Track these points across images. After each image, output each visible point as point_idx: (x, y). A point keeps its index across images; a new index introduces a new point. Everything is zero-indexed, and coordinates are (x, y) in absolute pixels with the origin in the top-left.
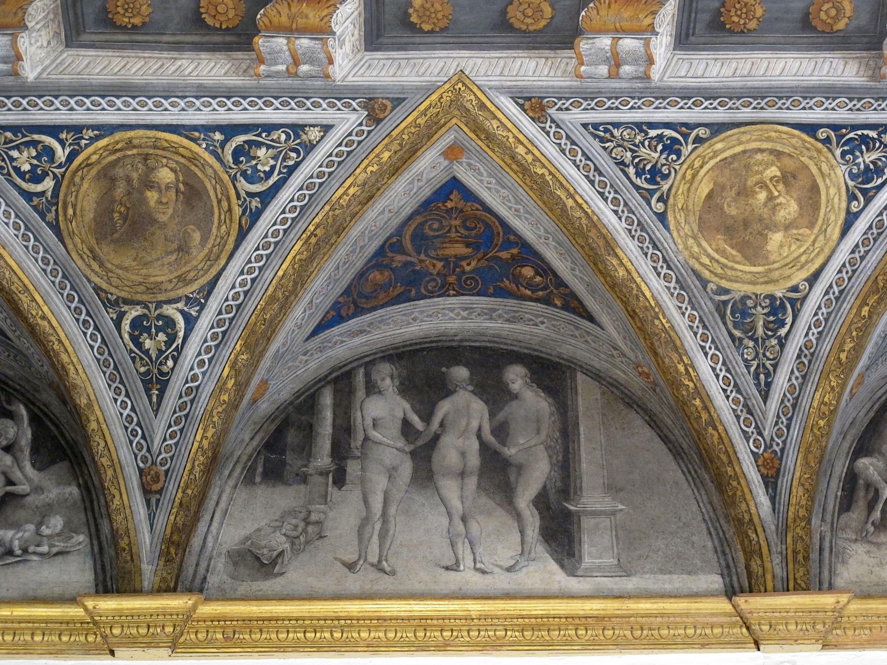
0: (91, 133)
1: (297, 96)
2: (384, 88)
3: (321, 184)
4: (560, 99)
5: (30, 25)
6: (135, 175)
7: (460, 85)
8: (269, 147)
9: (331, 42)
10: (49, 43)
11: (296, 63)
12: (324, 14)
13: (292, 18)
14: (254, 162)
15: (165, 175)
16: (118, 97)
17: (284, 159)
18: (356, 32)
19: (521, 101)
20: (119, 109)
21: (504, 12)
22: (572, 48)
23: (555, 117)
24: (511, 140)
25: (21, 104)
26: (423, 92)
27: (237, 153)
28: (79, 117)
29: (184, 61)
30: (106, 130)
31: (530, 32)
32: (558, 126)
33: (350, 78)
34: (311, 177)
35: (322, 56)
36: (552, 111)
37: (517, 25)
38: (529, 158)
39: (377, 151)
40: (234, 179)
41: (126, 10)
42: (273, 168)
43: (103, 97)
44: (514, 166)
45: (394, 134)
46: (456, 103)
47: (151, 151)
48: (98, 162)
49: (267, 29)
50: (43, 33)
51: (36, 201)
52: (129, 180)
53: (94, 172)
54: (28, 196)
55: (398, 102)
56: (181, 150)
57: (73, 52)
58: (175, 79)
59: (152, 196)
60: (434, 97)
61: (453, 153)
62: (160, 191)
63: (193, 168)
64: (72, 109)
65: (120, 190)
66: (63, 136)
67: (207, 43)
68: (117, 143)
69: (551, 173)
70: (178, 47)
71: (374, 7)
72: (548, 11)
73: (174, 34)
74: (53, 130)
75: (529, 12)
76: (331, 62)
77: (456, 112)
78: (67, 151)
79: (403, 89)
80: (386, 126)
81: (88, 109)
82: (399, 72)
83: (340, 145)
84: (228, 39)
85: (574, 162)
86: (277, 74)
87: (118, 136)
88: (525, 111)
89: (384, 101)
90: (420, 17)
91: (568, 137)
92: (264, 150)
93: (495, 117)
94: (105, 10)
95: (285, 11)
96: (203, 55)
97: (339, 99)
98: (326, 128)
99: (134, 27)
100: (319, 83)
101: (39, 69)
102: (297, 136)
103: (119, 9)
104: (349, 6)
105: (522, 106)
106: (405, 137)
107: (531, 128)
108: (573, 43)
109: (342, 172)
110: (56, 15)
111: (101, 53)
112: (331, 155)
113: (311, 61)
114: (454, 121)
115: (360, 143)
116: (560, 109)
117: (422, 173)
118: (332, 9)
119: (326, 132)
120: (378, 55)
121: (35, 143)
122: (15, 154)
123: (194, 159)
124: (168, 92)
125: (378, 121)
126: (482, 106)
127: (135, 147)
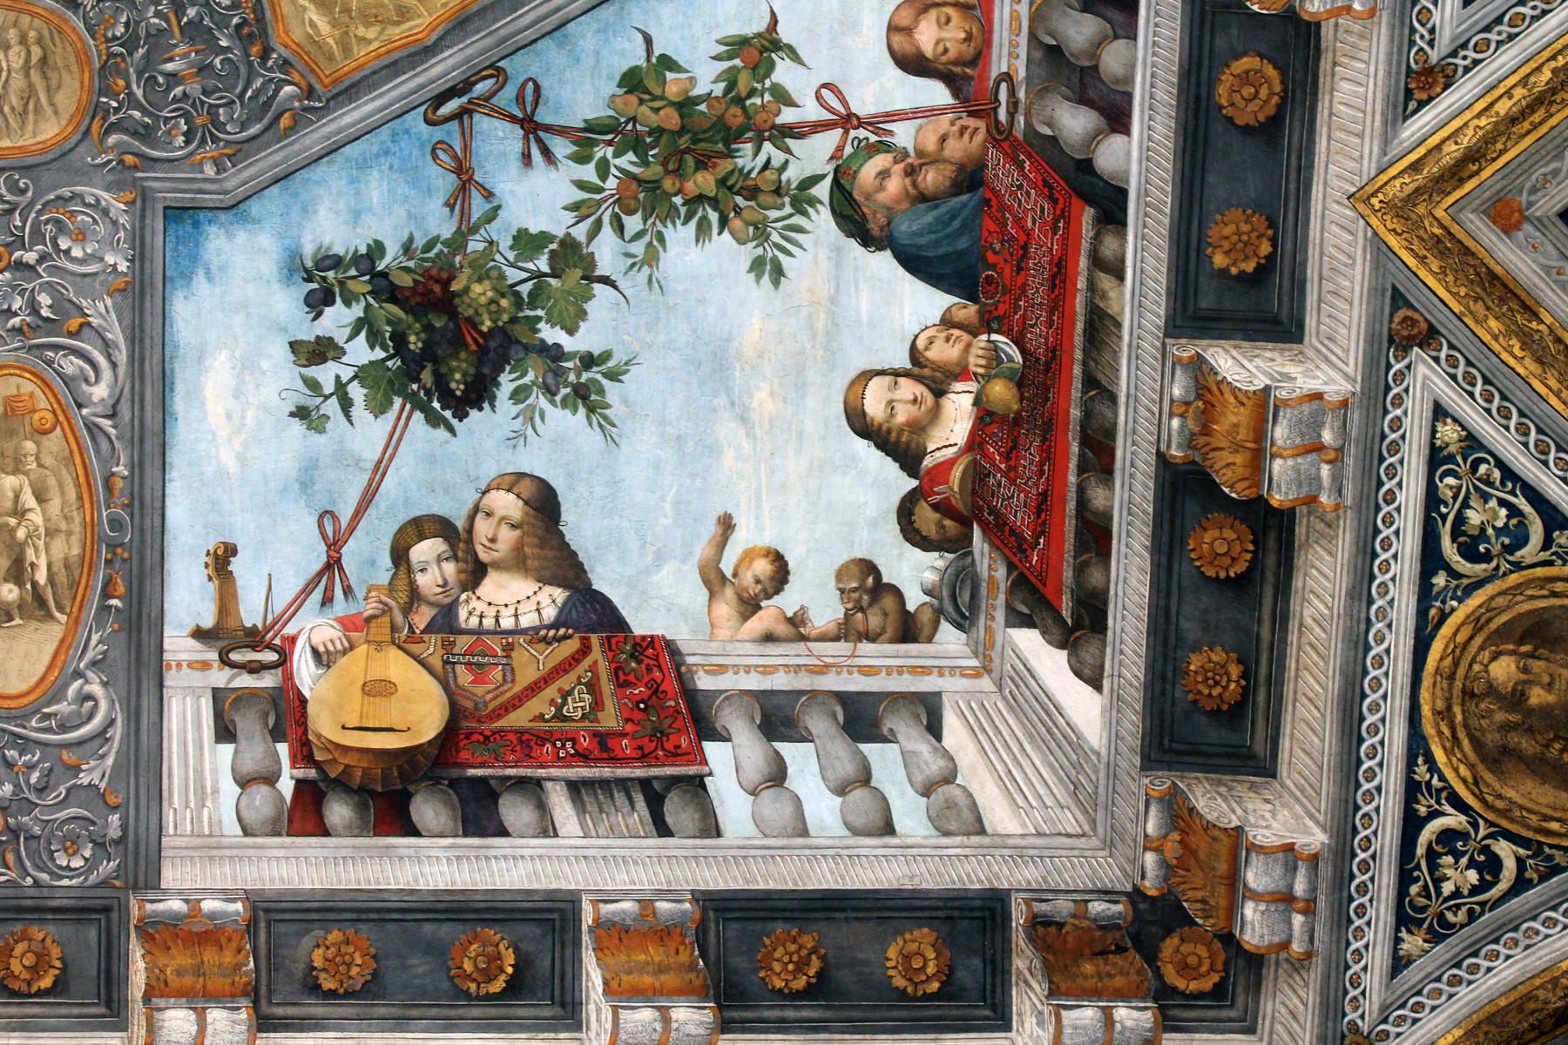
0: (1421, 769)
1: (1377, 455)
2: (1373, 319)
3: (1540, 431)
4: (1412, 43)
5: (1235, 823)
6: (1500, 717)
7: (1374, 201)
8: (1465, 505)
9: (1283, 394)
10: (1267, 801)
11: (1319, 448)
12: (1232, 399)
13: (1237, 447)
14: (1490, 531)
15: (1503, 670)
16: (1362, 719)
17: (1490, 484)
18: (1268, 354)
19: (1412, 105)
20: (1383, 720)
21: (1247, 130)
22: (1318, 25)
23: (1445, 51)
24: (1483, 122)
25: (1364, 860)
26: (1382, 257)
27: (1470, 554)
28: (1392, 780)
29: (1306, 613)
30: (1417, 745)
31: (1285, 90)
32: (1464, 46)
33: (1350, 370)
34: (1526, 445)
35: (1306, 408)
36: (1434, 56)
37: (1271, 110)
38: (1519, 93)
39: (1487, 338)
40: (1518, 566)
41: (1217, 683)
42: (1502, 503)
43: (1361, 740)
44: (1536, 118)
45: (1457, 308)
46: (1402, 209)
47: (1458, 684)
48: (1471, 767)
49: (1258, 485)
50: (1250, 807)
51: (1530, 874)
52: (1507, 727)
53: (1489, 777)
54: (1521, 884)
55: (1398, 300)
56: (1460, 638)
57: (1283, 769)
58: (1337, 629)
59: (1537, 696)
60: (1393, 241)
61: (1506, 216)
62: (1530, 682)
63: (1493, 626)
64: (1379, 789)
65: (1527, 745)
66: (1423, 810)
67: (1277, 575)
68: (1440, 733)
69: (1553, 58)
70: (1281, 618)
71: (1222, 325)
72: (1246, 63)
73: (1259, 621)
74: (1412, 824)
75: (1248, 91)
76: (1318, 396)
77: (1421, 209)
78: (1448, 808)
79: (1375, 290)
80: (1441, 319)
81: (1381, 765)
82: (1345, 293)
83: (1471, 395)
84: (1271, 543)
85: (1535, 18)
86: (1337, 480)
87: (1429, 729)
88: (1431, 99)
89: (1396, 320)
90: (1246, 258)
91: (1487, 29)
92: (1469, 513)
93: (1438, 147)
94: (1216, 713)
95: (1225, 457)
96: (1297, 583)
97: (1388, 388)
98: (1440, 412)
99: (1245, 675)
100: (1355, 417)
101: (1310, 823)
102: (1451, 458)
103: (1215, 692)
104: (1222, 362)
105: (1422, 104)
106: (1463, 292)
107: (1464, 90)
108: (1308, 24)
109: (1520, 395)
110: (1220, 783)
111: (1286, 729)
112: (1488, 411)
113: (1317, 426)
114: (1439, 213)
115: (1469, 363)
116: (1431, 43)
117: (1547, 269)
118: (1224, 387)
119: (1446, 414)
120: (1310, 322)
121: (1431, 855)
122: (1447, 888)
123: (1477, 622)
124: (1358, 644)
125: (1433, 332)
126: (1415, 167)
127: (1449, 708)
